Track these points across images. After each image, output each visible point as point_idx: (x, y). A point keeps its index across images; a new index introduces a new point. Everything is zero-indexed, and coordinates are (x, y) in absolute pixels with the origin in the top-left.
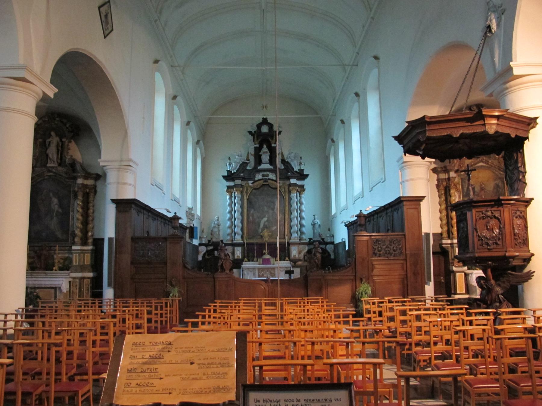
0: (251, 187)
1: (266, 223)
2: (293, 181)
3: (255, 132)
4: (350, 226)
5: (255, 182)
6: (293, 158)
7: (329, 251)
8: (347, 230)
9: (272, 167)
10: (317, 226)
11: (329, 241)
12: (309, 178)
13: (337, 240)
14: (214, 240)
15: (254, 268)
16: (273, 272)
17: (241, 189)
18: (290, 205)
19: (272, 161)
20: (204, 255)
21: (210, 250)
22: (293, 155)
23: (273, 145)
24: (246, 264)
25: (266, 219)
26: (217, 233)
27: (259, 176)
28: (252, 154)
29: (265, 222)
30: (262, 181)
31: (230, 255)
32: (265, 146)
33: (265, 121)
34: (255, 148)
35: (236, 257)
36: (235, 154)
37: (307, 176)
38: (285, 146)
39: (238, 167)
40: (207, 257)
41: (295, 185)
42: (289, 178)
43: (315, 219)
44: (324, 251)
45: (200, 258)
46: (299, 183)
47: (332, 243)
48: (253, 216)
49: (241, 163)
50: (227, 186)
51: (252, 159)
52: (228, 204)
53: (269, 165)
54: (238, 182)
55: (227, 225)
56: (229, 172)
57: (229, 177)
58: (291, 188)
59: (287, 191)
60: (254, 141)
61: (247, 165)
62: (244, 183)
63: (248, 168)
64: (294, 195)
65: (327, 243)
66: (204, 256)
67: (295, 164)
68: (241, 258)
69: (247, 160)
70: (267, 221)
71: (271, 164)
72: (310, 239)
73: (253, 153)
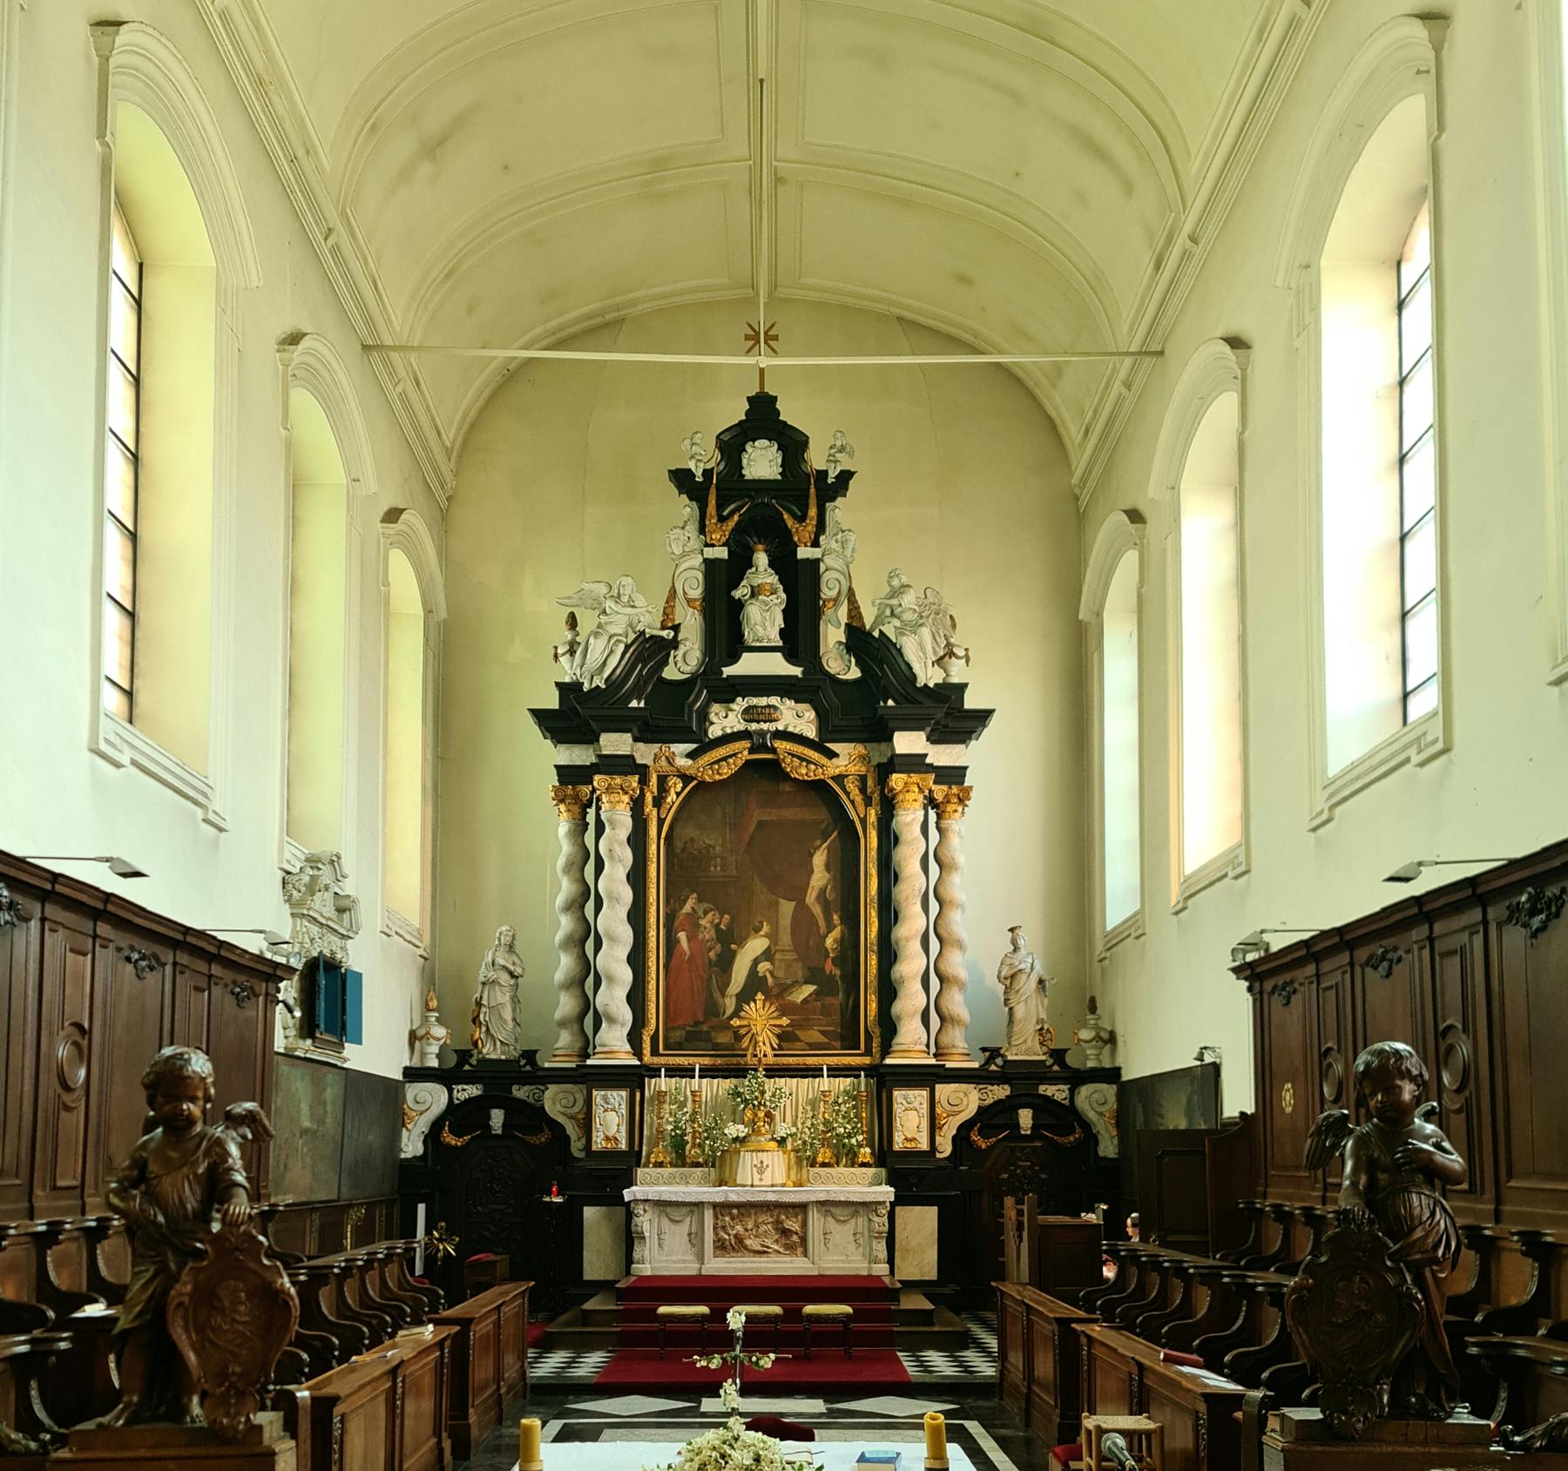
0: (686, 778)
1: (764, 967)
2: (907, 742)
3: (707, 473)
4: (1265, 973)
5: (706, 746)
6: (908, 616)
7: (1092, 1116)
8: (1247, 1000)
9: (797, 671)
10: (1028, 985)
11: (1091, 1064)
12: (994, 722)
13: (1144, 1058)
14: (491, 1052)
15: (698, 1206)
16: (793, 1224)
17: (634, 781)
18: (889, 874)
19: (799, 637)
20: (437, 1126)
21: (470, 1101)
22: (909, 600)
23: (804, 553)
24: (647, 1186)
25: (756, 945)
26: (507, 1014)
27: (725, 720)
28: (689, 601)
29: (756, 962)
30: (747, 744)
31: (571, 1130)
32: (761, 559)
33: (763, 417)
34: (709, 564)
35: (599, 1143)
36: (603, 589)
37: (983, 716)
38: (866, 558)
39: (613, 662)
40: (450, 1139)
41: (916, 763)
42: (880, 733)
43: (1016, 949)
44: (1068, 1116)
45: (412, 1145)
46: (942, 755)
47: (1111, 1075)
48: (693, 924)
49: (632, 636)
50: (560, 769)
51: (691, 625)
52: (561, 862)
53: (779, 655)
54: (616, 743)
55: (559, 976)
56: (568, 690)
57: (572, 716)
58: (897, 780)
59: (876, 797)
60: (702, 530)
61: (665, 662)
62: (645, 753)
63: (670, 673)
64: (910, 817)
65: (1077, 1078)
66: (432, 1136)
67: (922, 648)
68: (623, 1146)
69: (663, 628)
70: (768, 955)
71: (791, 656)
72: (993, 1053)
73: (696, 593)
